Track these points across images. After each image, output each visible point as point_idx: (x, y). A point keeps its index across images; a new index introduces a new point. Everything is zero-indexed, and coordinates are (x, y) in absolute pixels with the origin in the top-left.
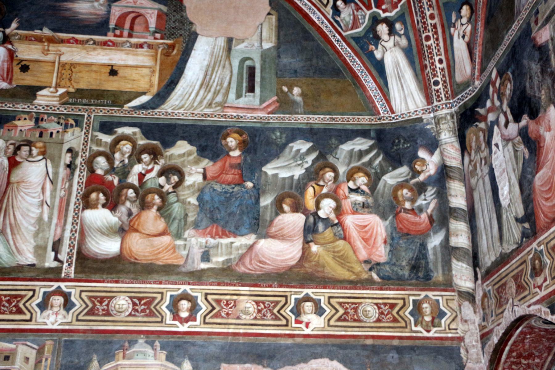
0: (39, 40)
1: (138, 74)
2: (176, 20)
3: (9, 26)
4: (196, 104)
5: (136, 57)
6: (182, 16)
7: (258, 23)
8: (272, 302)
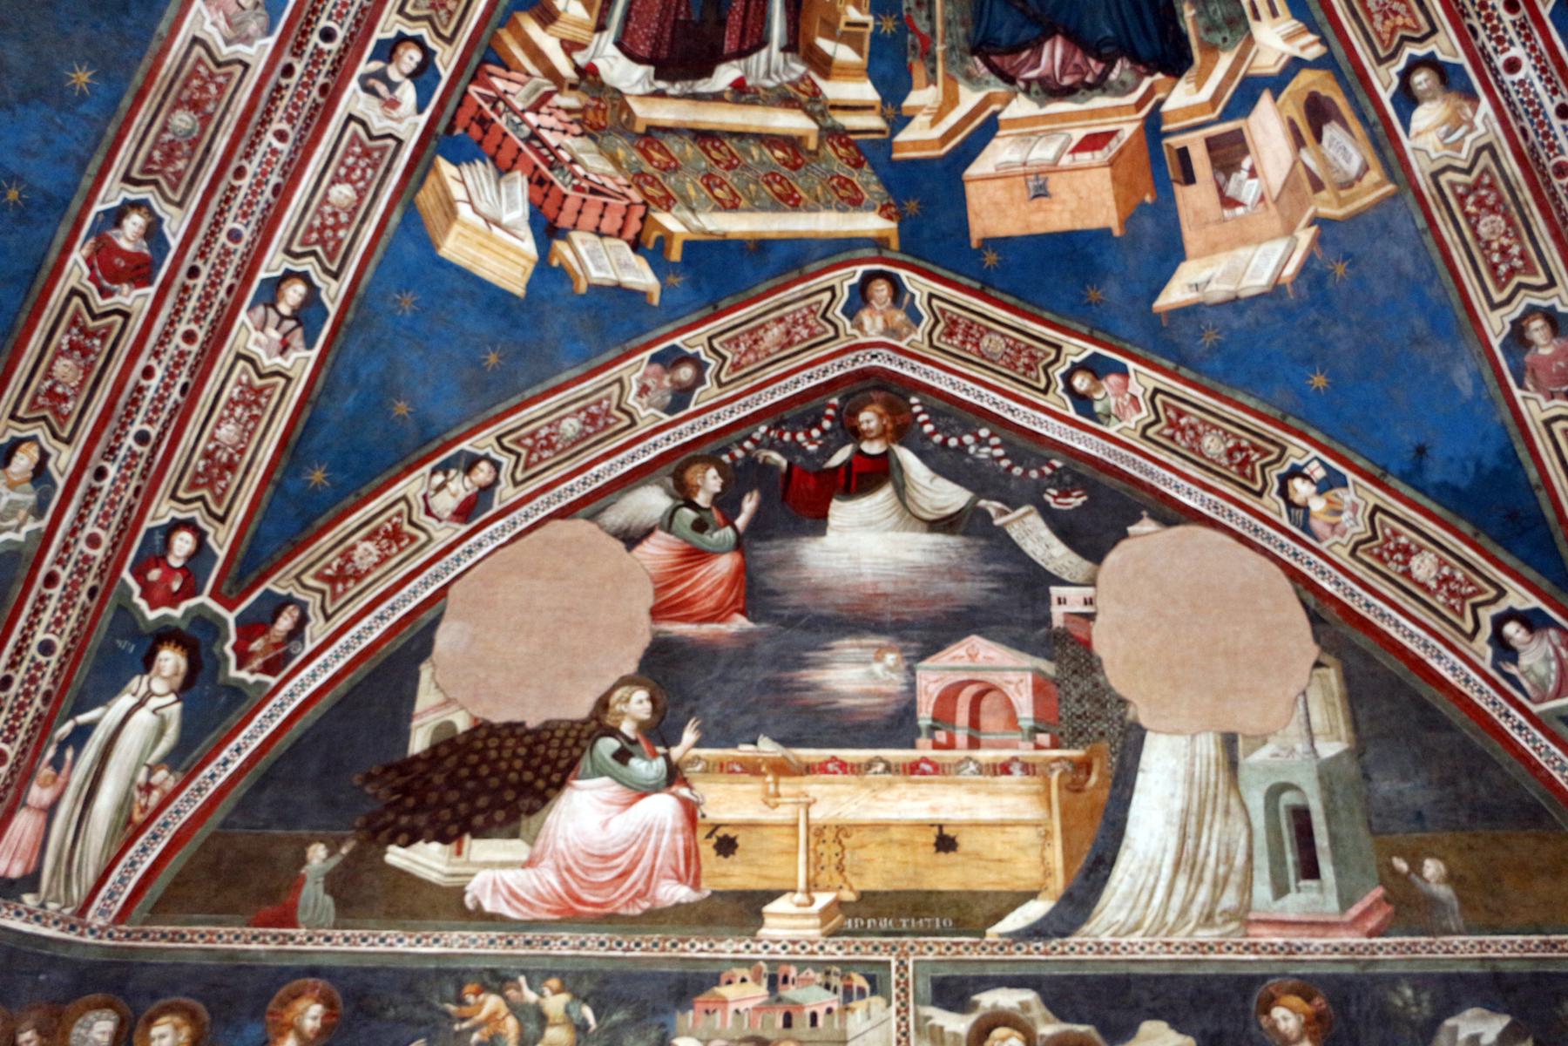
0: (752, 769)
1: (1010, 843)
2: (1082, 696)
3: (676, 741)
4: (1171, 917)
5: (996, 800)
6: (1096, 685)
7: (1293, 691)
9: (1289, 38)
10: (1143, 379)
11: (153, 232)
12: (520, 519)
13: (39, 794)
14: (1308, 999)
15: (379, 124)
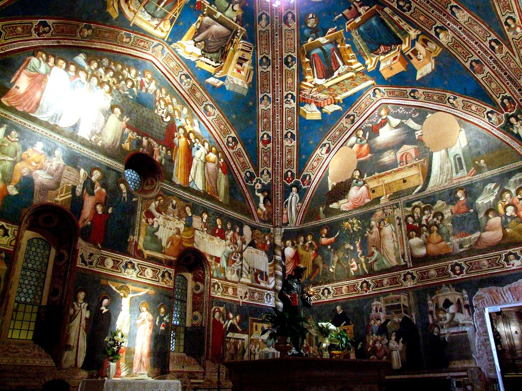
0: (375, 178)
8: (494, 259)
9: (415, 32)
10: (421, 91)
11: (268, 136)
12: (336, 149)
13: (285, 212)
14: (462, 190)
15: (290, 107)
